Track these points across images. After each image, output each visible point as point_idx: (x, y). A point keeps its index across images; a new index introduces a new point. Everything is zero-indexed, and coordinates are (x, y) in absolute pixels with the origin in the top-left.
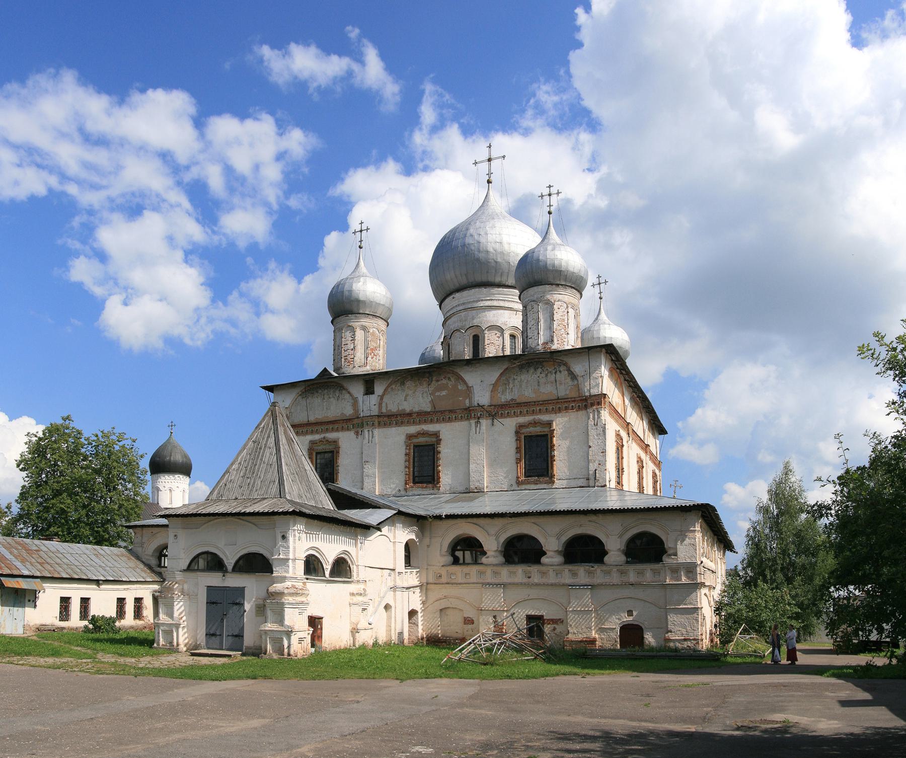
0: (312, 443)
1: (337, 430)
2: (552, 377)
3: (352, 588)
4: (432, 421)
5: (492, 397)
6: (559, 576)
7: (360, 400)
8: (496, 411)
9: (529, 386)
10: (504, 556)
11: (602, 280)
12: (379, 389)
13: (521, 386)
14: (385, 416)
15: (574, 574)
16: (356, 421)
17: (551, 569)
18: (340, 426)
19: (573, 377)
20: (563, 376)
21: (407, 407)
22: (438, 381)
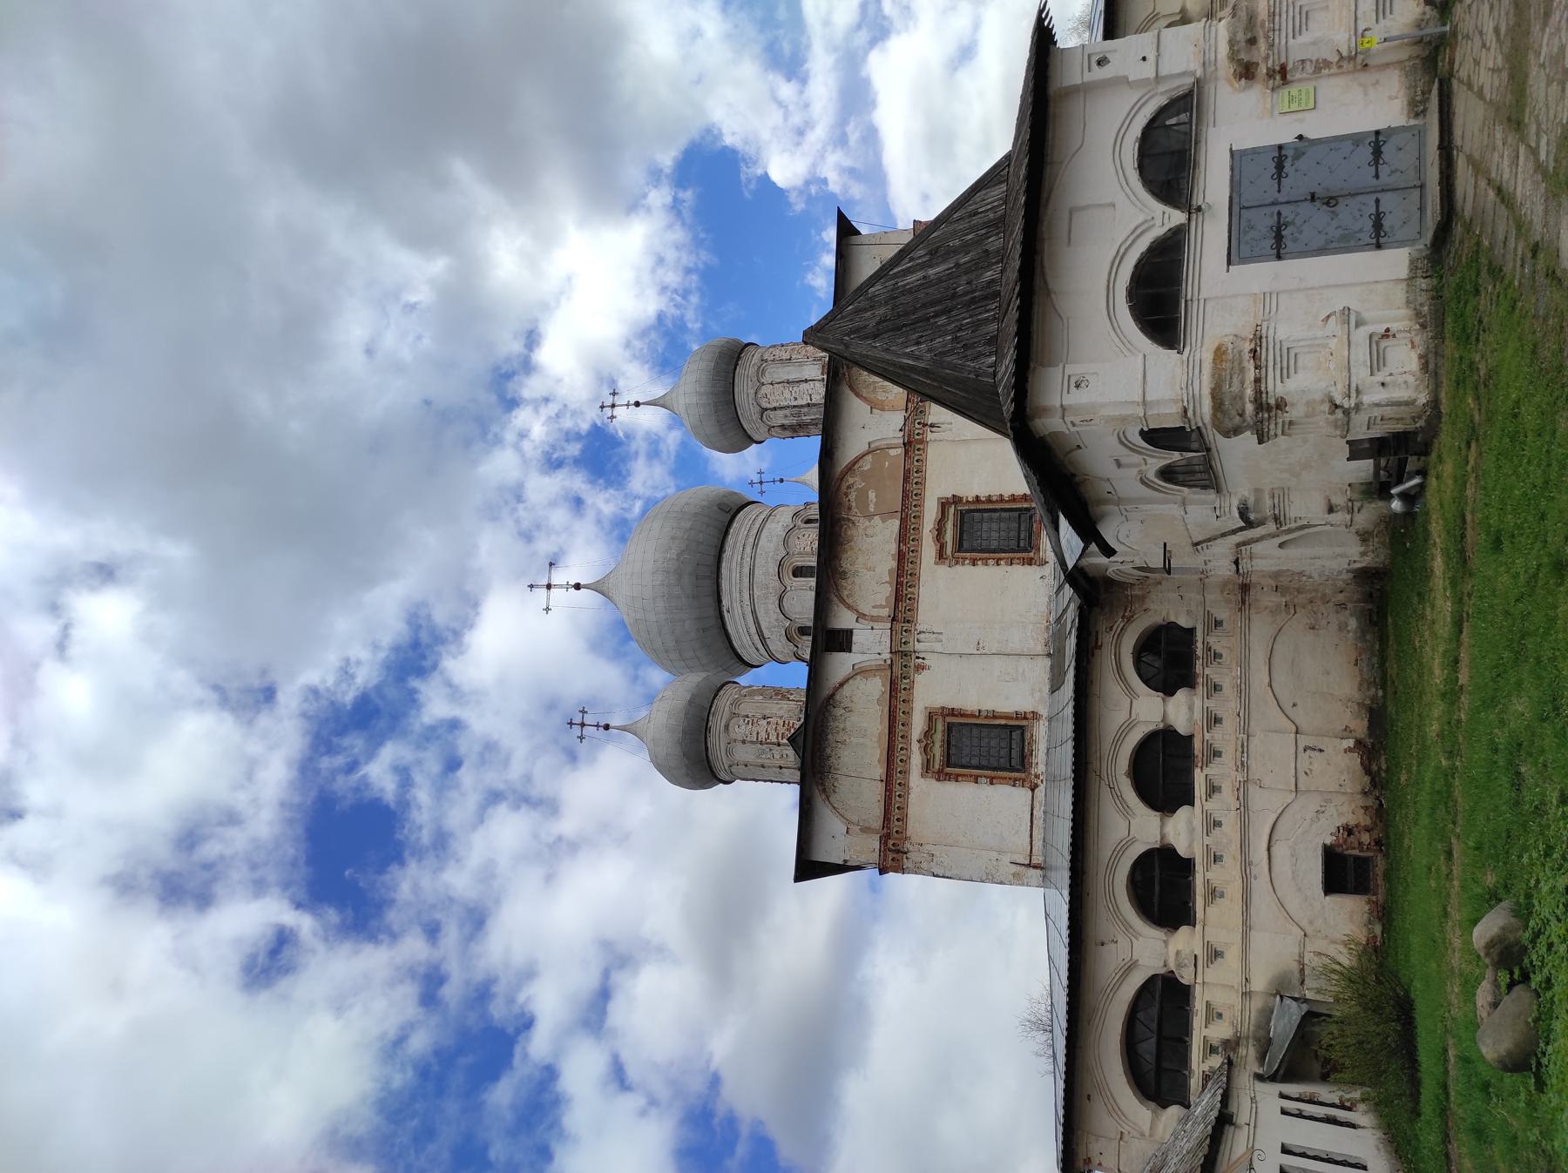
5: (893, 409)
12: (843, 619)
18: (902, 706)
21: (885, 564)
22: (850, 509)
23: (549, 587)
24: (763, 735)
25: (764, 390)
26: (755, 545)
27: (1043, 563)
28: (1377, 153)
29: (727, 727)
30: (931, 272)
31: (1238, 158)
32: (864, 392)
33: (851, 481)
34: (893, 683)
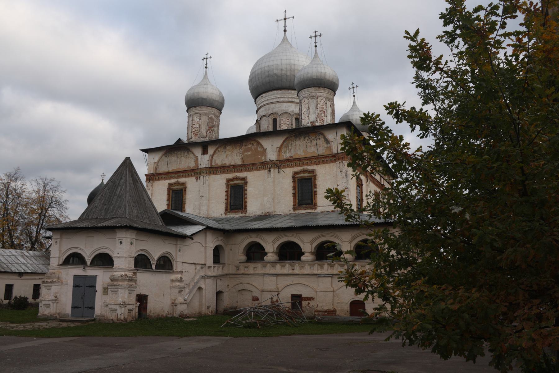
0: (170, 185)
1: (185, 177)
2: (314, 143)
3: (173, 277)
4: (242, 171)
5: (279, 155)
6: (312, 268)
7: (199, 158)
8: (280, 164)
9: (301, 148)
10: (279, 256)
11: (355, 86)
12: (211, 151)
13: (296, 148)
14: (214, 168)
15: (321, 267)
16: (197, 171)
17: (306, 264)
18: (187, 174)
19: (327, 142)
20: (321, 141)
22: (246, 146)
23: (285, 19)
24: (194, 126)
25: (306, 100)
26: (284, 102)
27: (226, 214)
28: (90, 308)
29: (196, 113)
30: (116, 197)
31: (95, 277)
32: (285, 143)
33: (255, 144)
34: (193, 170)
